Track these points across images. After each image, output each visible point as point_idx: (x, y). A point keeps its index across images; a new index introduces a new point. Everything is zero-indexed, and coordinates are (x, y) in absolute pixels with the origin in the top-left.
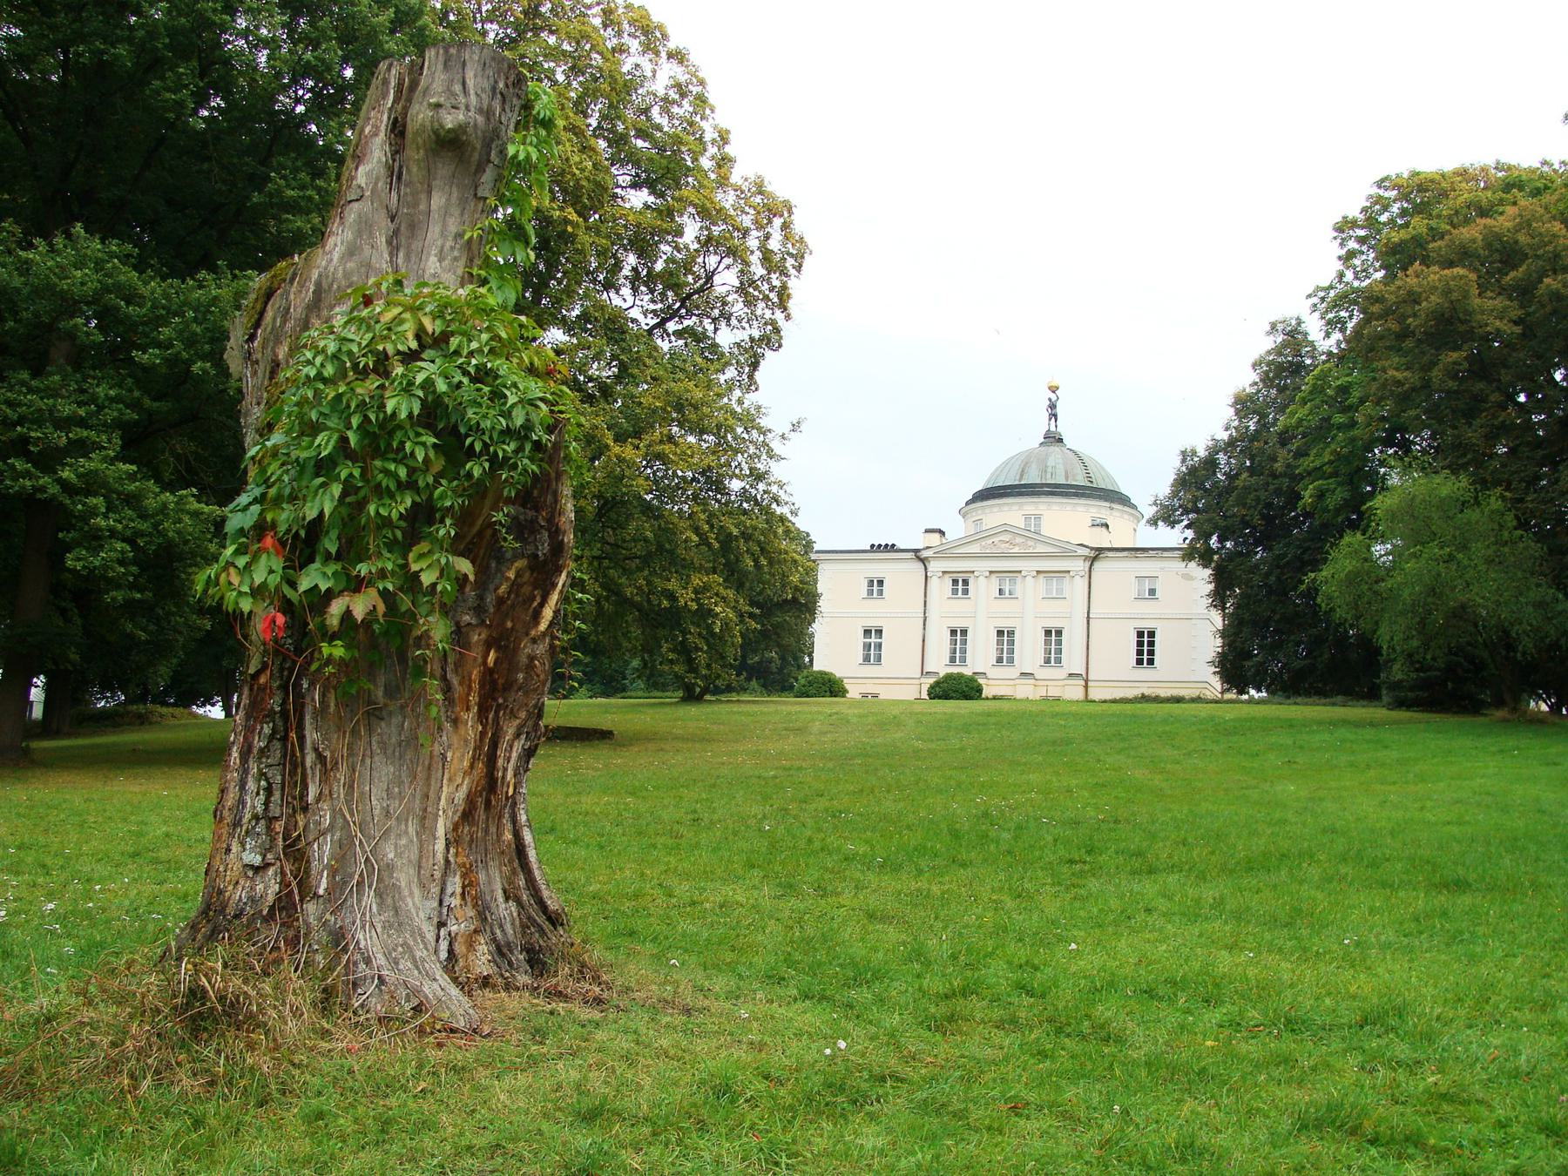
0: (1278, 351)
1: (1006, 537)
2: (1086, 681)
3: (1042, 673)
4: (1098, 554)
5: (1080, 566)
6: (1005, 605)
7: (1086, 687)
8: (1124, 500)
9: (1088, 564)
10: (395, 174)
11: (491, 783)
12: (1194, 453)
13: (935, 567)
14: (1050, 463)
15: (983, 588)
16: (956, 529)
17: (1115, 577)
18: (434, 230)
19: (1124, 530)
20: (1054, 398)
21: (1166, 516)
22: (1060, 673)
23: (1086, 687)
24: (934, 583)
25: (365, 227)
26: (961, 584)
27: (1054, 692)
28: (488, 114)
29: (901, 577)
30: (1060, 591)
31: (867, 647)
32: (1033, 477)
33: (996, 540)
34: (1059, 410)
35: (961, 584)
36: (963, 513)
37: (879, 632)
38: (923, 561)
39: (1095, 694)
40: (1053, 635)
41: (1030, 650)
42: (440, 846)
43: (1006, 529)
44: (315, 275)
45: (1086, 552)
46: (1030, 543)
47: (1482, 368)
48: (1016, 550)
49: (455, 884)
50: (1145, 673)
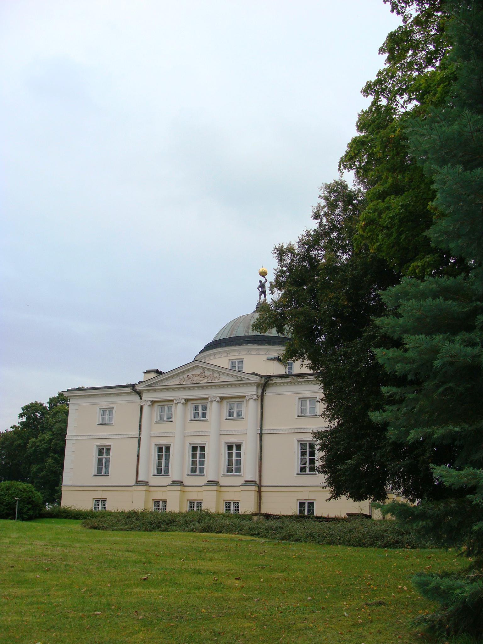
1: (198, 372)
2: (260, 486)
4: (266, 382)
5: (252, 391)
6: (198, 427)
7: (259, 492)
9: (260, 391)
13: (147, 397)
20: (263, 280)
22: (239, 481)
23: (259, 492)
31: (100, 461)
33: (190, 374)
37: (108, 450)
38: (140, 394)
45: (256, 379)
46: (216, 375)
48: (205, 381)
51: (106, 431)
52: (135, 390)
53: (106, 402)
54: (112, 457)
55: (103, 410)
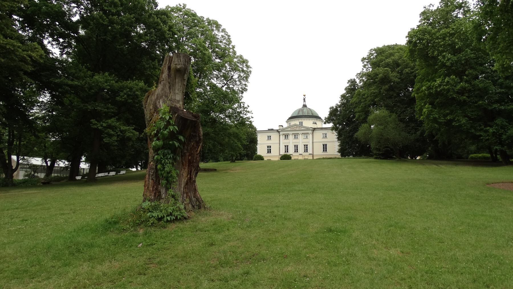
0: (350, 86)
3: (304, 154)
4: (314, 129)
5: (310, 132)
8: (320, 118)
10: (169, 76)
11: (190, 178)
12: (333, 107)
13: (281, 133)
14: (304, 111)
15: (291, 137)
16: (285, 125)
17: (318, 135)
18: (177, 85)
19: (320, 124)
21: (328, 120)
24: (281, 136)
25: (164, 85)
26: (286, 136)
27: (306, 158)
28: (185, 65)
29: (275, 136)
30: (307, 137)
32: (301, 114)
35: (286, 136)
36: (287, 122)
37: (270, 147)
38: (279, 132)
39: (315, 158)
40: (306, 146)
41: (301, 149)
42: (182, 189)
43: (295, 125)
44: (156, 94)
47: (391, 89)
49: (185, 195)
50: (325, 153)
51: (269, 142)
52: (278, 131)
53: (269, 134)
54: (271, 148)
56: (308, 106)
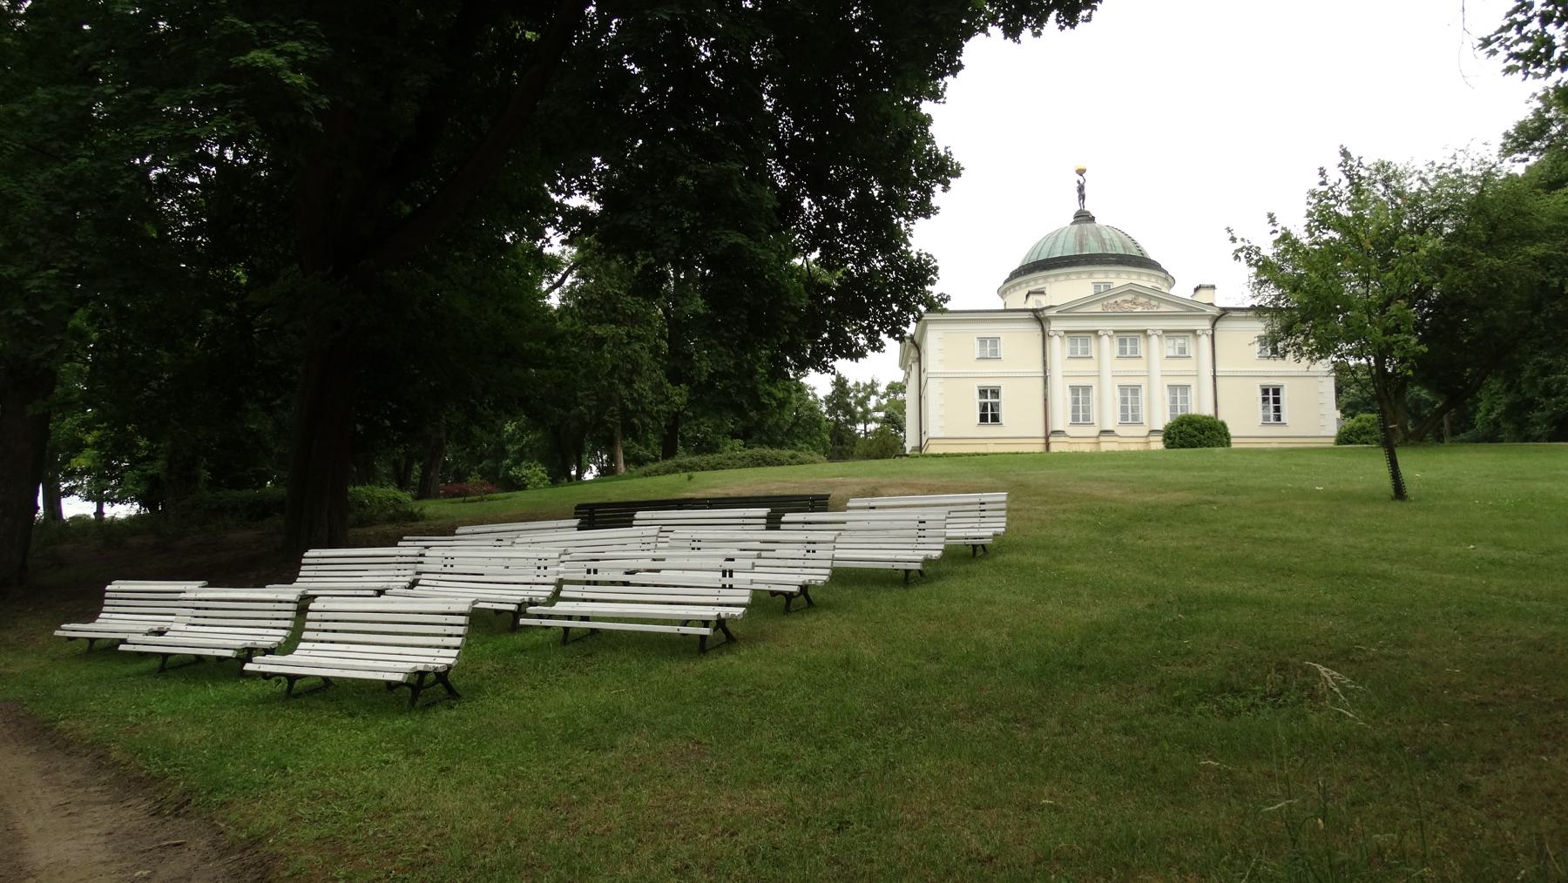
1: (1129, 297)
5: (1205, 325)
13: (1055, 326)
31: (984, 407)
33: (1119, 299)
34: (1087, 191)
37: (996, 393)
55: (983, 341)
56: (1100, 221)
